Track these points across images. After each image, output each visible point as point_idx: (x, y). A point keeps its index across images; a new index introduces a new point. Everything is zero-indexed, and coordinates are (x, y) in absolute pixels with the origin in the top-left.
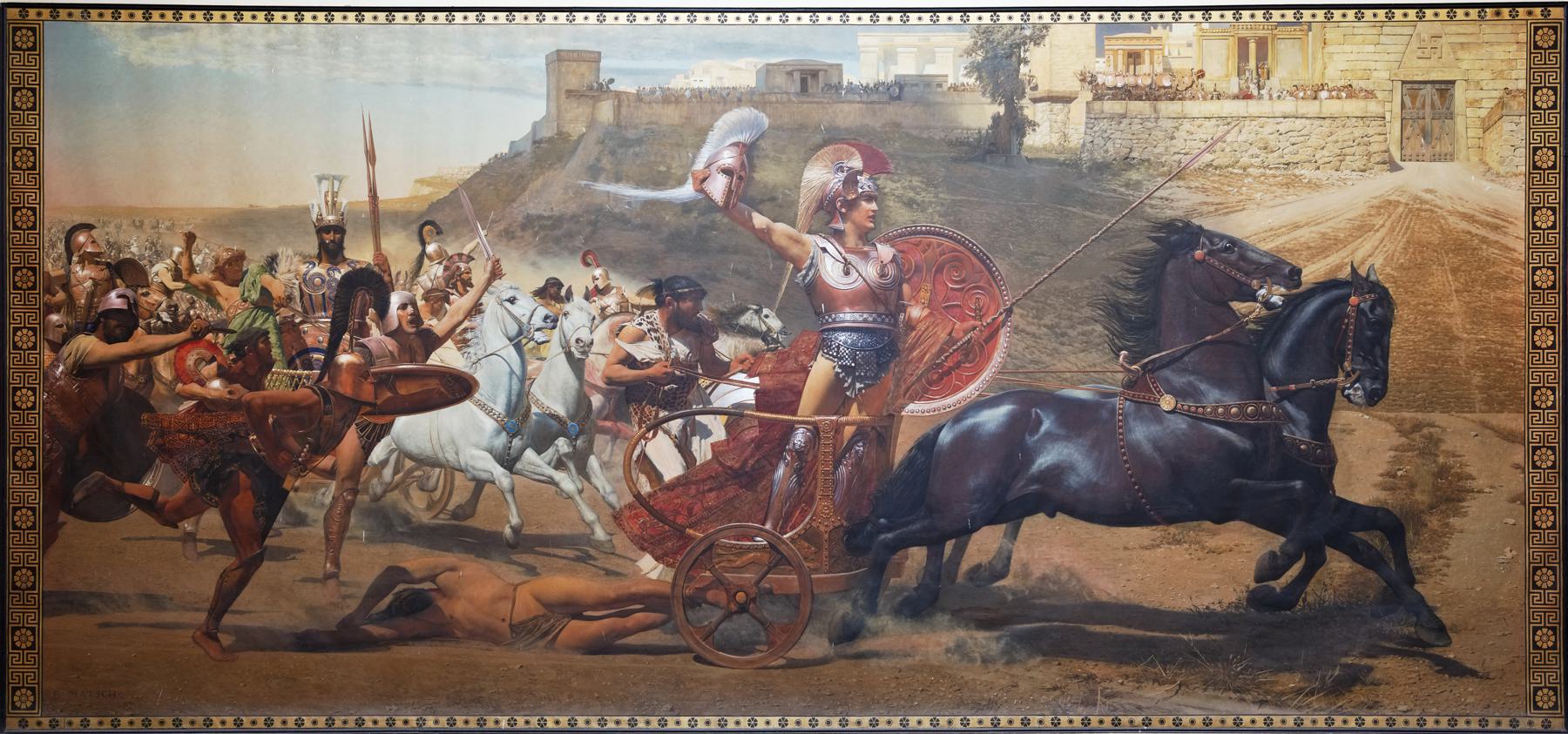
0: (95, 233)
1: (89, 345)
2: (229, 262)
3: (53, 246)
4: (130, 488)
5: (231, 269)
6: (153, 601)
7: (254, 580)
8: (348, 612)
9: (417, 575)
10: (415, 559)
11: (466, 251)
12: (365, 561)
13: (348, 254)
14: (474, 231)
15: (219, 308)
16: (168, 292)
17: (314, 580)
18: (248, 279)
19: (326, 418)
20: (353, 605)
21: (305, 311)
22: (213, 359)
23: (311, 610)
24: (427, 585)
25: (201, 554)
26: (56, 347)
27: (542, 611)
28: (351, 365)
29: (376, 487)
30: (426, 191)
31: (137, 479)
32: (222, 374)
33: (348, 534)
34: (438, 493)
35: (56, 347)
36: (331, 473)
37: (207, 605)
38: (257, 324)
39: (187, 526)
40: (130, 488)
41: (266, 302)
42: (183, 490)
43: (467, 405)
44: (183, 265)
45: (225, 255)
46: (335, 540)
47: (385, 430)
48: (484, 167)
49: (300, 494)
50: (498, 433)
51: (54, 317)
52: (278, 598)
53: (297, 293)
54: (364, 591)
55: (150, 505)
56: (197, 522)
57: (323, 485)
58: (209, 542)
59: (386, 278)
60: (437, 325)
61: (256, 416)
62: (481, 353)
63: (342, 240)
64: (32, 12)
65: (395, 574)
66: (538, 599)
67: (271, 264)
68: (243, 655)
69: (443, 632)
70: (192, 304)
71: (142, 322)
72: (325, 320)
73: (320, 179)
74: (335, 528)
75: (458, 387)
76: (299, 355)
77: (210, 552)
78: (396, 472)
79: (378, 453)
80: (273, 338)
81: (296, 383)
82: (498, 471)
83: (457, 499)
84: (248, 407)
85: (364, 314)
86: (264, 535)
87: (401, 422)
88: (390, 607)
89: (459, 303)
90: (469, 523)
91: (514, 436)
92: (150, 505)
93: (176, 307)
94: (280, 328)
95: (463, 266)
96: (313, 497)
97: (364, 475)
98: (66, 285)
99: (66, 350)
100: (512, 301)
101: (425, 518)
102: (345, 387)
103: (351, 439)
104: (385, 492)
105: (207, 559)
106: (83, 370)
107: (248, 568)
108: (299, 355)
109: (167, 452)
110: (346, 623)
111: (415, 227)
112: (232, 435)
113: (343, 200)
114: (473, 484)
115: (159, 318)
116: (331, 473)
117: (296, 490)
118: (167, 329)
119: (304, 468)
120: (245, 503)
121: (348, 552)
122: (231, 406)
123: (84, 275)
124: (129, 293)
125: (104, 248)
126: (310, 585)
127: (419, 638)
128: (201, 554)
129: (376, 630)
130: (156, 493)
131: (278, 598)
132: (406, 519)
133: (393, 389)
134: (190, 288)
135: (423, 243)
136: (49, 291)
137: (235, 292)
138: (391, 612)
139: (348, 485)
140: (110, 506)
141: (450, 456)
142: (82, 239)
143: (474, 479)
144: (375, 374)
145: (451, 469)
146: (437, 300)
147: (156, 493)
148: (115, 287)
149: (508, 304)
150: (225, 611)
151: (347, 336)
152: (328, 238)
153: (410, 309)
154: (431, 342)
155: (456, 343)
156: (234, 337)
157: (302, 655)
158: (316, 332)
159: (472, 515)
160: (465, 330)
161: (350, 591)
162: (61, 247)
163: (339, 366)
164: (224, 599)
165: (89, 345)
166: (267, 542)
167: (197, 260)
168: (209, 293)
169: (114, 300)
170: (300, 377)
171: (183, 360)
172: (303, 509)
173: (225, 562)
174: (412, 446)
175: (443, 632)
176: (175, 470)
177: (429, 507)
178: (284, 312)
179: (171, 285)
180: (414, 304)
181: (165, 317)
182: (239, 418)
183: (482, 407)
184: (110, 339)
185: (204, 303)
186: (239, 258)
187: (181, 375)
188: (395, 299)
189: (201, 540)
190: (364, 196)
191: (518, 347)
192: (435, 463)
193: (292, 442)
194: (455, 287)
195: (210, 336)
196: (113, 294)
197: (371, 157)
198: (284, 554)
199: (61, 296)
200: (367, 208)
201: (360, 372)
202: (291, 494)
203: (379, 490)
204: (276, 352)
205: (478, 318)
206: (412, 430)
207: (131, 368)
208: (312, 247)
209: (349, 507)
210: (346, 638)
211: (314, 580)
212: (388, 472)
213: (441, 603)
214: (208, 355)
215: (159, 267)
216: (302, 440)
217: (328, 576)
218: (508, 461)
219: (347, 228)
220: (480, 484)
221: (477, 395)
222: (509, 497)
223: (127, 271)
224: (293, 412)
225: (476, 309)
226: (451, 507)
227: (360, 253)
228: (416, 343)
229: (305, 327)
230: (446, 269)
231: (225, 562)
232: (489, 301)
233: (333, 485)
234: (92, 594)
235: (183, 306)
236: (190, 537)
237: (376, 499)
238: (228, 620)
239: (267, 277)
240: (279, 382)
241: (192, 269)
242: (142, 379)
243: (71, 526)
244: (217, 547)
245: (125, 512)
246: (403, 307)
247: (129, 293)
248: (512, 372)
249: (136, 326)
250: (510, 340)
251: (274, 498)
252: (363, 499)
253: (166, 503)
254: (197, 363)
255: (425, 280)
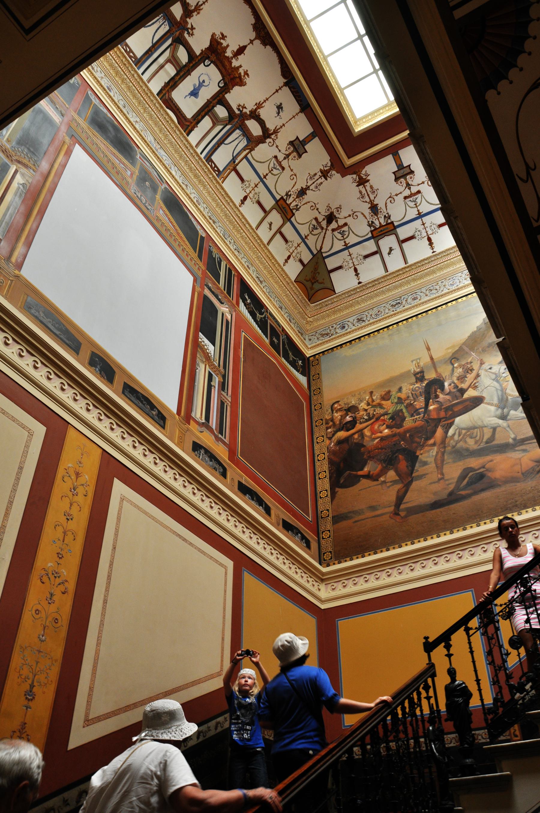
0: (340, 403)
1: (342, 434)
2: (385, 394)
3: (327, 411)
4: (360, 473)
5: (386, 396)
6: (373, 508)
7: (410, 489)
8: (450, 489)
9: (476, 468)
10: (474, 463)
11: (469, 361)
12: (453, 471)
13: (426, 378)
14: (471, 355)
15: (384, 408)
16: (366, 410)
17: (434, 483)
18: (392, 397)
19: (428, 428)
20: (452, 487)
21: (414, 399)
22: (384, 424)
23: (435, 493)
24: (482, 470)
25: (389, 487)
26: (330, 438)
27: (535, 464)
28: (434, 409)
29: (452, 443)
30: (450, 351)
31: (362, 469)
32: (388, 427)
33: (445, 463)
34: (478, 438)
35: (330, 438)
36: (434, 444)
37: (394, 504)
38: (398, 408)
39: (382, 479)
40: (360, 473)
41: (400, 401)
42: (379, 467)
43: (482, 405)
44: (370, 401)
45: (384, 393)
46: (440, 467)
47: (452, 424)
48: (469, 337)
49: (423, 455)
50: (497, 410)
51: (329, 430)
52: (422, 492)
53: (410, 395)
54: (456, 480)
55: (368, 476)
56: (386, 476)
57: (432, 449)
58: (391, 482)
59: (442, 379)
60: (464, 386)
61: (402, 436)
62: (483, 388)
63: (423, 375)
64: (317, 356)
65: (466, 472)
66: (533, 461)
67: (400, 390)
68: (410, 517)
69: (492, 485)
70: (375, 411)
71: (358, 422)
72: (422, 399)
73: (412, 361)
74: (439, 462)
75: (477, 401)
76: (414, 412)
77: (392, 485)
78: (459, 435)
79: (451, 432)
80: (404, 410)
81: (415, 421)
82: (501, 422)
83: (487, 435)
84: (399, 434)
85: (436, 392)
86: (412, 473)
87: (458, 420)
88: (468, 482)
89: (470, 377)
90: (495, 442)
91: (503, 409)
92: (368, 476)
93: (369, 413)
94: (406, 407)
95: (469, 366)
96: (428, 455)
97: (447, 440)
98: (332, 420)
99: (333, 439)
100: (490, 369)
101: (476, 447)
102: (434, 415)
103: (440, 431)
104: (456, 444)
105: (391, 488)
106: (340, 442)
107: (407, 487)
108: (414, 412)
109: (371, 458)
110: (451, 494)
111: (449, 362)
112: (394, 445)
113: (422, 364)
114: (492, 430)
115: (364, 418)
116: (434, 444)
117: (421, 454)
118: (367, 421)
119: (423, 446)
120: (403, 465)
121: (446, 469)
122: (394, 435)
123: (337, 416)
124: (353, 415)
125: (343, 405)
126: (433, 484)
127: (483, 490)
128: (389, 487)
129: (463, 493)
130: (370, 472)
131: (422, 492)
132: (467, 450)
133: (452, 410)
134: (374, 406)
135: (453, 365)
136: (327, 423)
137: (389, 402)
138: (469, 484)
139: (442, 446)
140: (353, 481)
141: (480, 423)
142: (336, 406)
143: (492, 428)
144: (444, 408)
145: (481, 428)
146: (462, 378)
147: (370, 472)
148: (348, 415)
149: (489, 370)
150: (400, 504)
151: (431, 401)
152: (418, 376)
153: (453, 385)
154: (462, 391)
155: (473, 388)
156: (390, 415)
157: (434, 511)
158: (420, 403)
159: (494, 440)
160: (475, 383)
161: (450, 482)
162: (330, 410)
163: (430, 411)
164: (400, 499)
165: (342, 434)
166: (413, 475)
167: (374, 398)
168: (380, 406)
169: (348, 419)
170: (416, 419)
171: (374, 428)
172: (425, 460)
173: (399, 486)
174: (463, 425)
175: (492, 485)
176: (375, 462)
177: (476, 442)
178: (407, 402)
179: (366, 407)
180: (454, 383)
181: (366, 417)
182: (395, 439)
183: (488, 404)
184: (348, 430)
185: (379, 409)
186: (389, 392)
187: (373, 432)
188: (446, 384)
189: (388, 482)
190: (428, 359)
191: (497, 381)
192: (474, 428)
193: (417, 440)
194: (468, 372)
195: (382, 418)
196: (348, 417)
197: (428, 349)
198: (420, 477)
199: (331, 423)
200: (430, 363)
201: (438, 410)
202: (420, 456)
203: (454, 444)
204: (406, 414)
205: (479, 378)
206: (461, 421)
207: (356, 436)
208: (413, 379)
209: (443, 454)
210: (453, 498)
211: (434, 483)
212: (456, 437)
213: (489, 474)
214: (382, 423)
215: (362, 404)
216: (421, 438)
217: (440, 480)
218: (503, 417)
219: (425, 370)
220: (494, 429)
221: (485, 401)
222: (508, 429)
223: (352, 409)
224: (415, 431)
225: (478, 376)
226: (485, 440)
227: (431, 375)
228: (458, 394)
229: (415, 403)
230: (463, 369)
231: (399, 486)
232: (482, 373)
233: (436, 448)
234: (350, 512)
235: (371, 412)
236: (384, 482)
237: (454, 447)
238: (402, 506)
239: (399, 394)
240: (409, 422)
241: (373, 401)
242: (360, 438)
243: (340, 491)
244: (395, 482)
245: (359, 481)
246: (450, 385)
247: (353, 415)
248: (497, 390)
249: (356, 423)
250: (493, 380)
251: (412, 459)
252: (449, 449)
253: (373, 474)
254: (378, 427)
255: (456, 374)
